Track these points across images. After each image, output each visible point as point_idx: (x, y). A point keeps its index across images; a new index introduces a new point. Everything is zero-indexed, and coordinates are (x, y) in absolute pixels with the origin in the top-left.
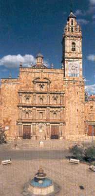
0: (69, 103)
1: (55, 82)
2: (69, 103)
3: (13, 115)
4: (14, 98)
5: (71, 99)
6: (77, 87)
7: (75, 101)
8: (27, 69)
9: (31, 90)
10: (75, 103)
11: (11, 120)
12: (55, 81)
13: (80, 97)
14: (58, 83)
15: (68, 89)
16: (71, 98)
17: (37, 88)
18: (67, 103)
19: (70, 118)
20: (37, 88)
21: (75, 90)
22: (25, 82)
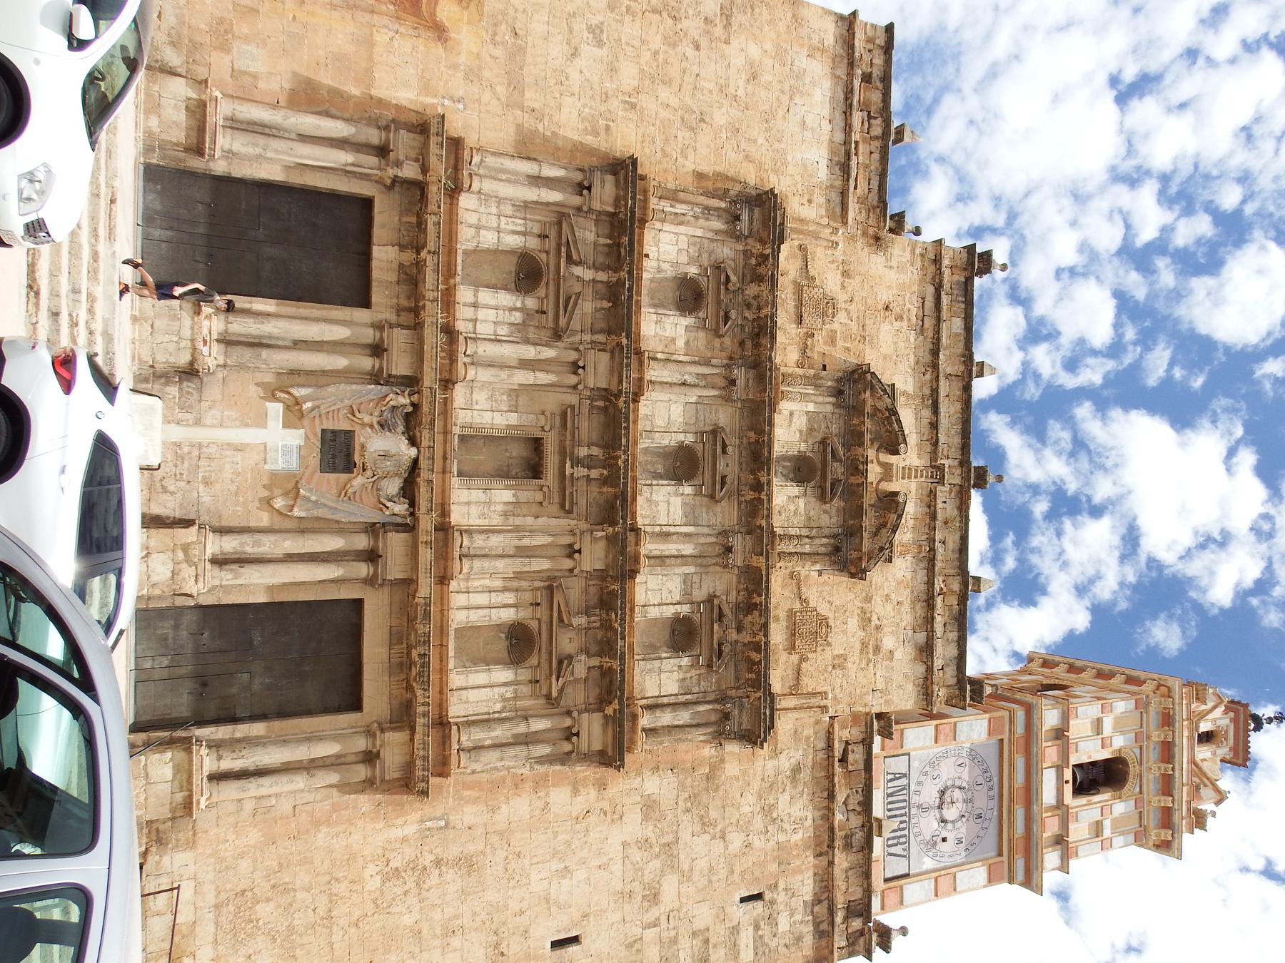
0: (650, 807)
1: (853, 623)
2: (650, 807)
3: (516, 85)
4: (705, 137)
5: (688, 826)
6: (806, 886)
7: (670, 886)
8: (957, 324)
9: (786, 354)
10: (653, 897)
11: (439, 31)
12: (865, 620)
13: (718, 934)
14: (839, 663)
15: (796, 770)
16: (705, 823)
17: (794, 424)
18: (653, 785)
19: (468, 864)
20: (794, 424)
21: (783, 856)
22: (853, 283)
